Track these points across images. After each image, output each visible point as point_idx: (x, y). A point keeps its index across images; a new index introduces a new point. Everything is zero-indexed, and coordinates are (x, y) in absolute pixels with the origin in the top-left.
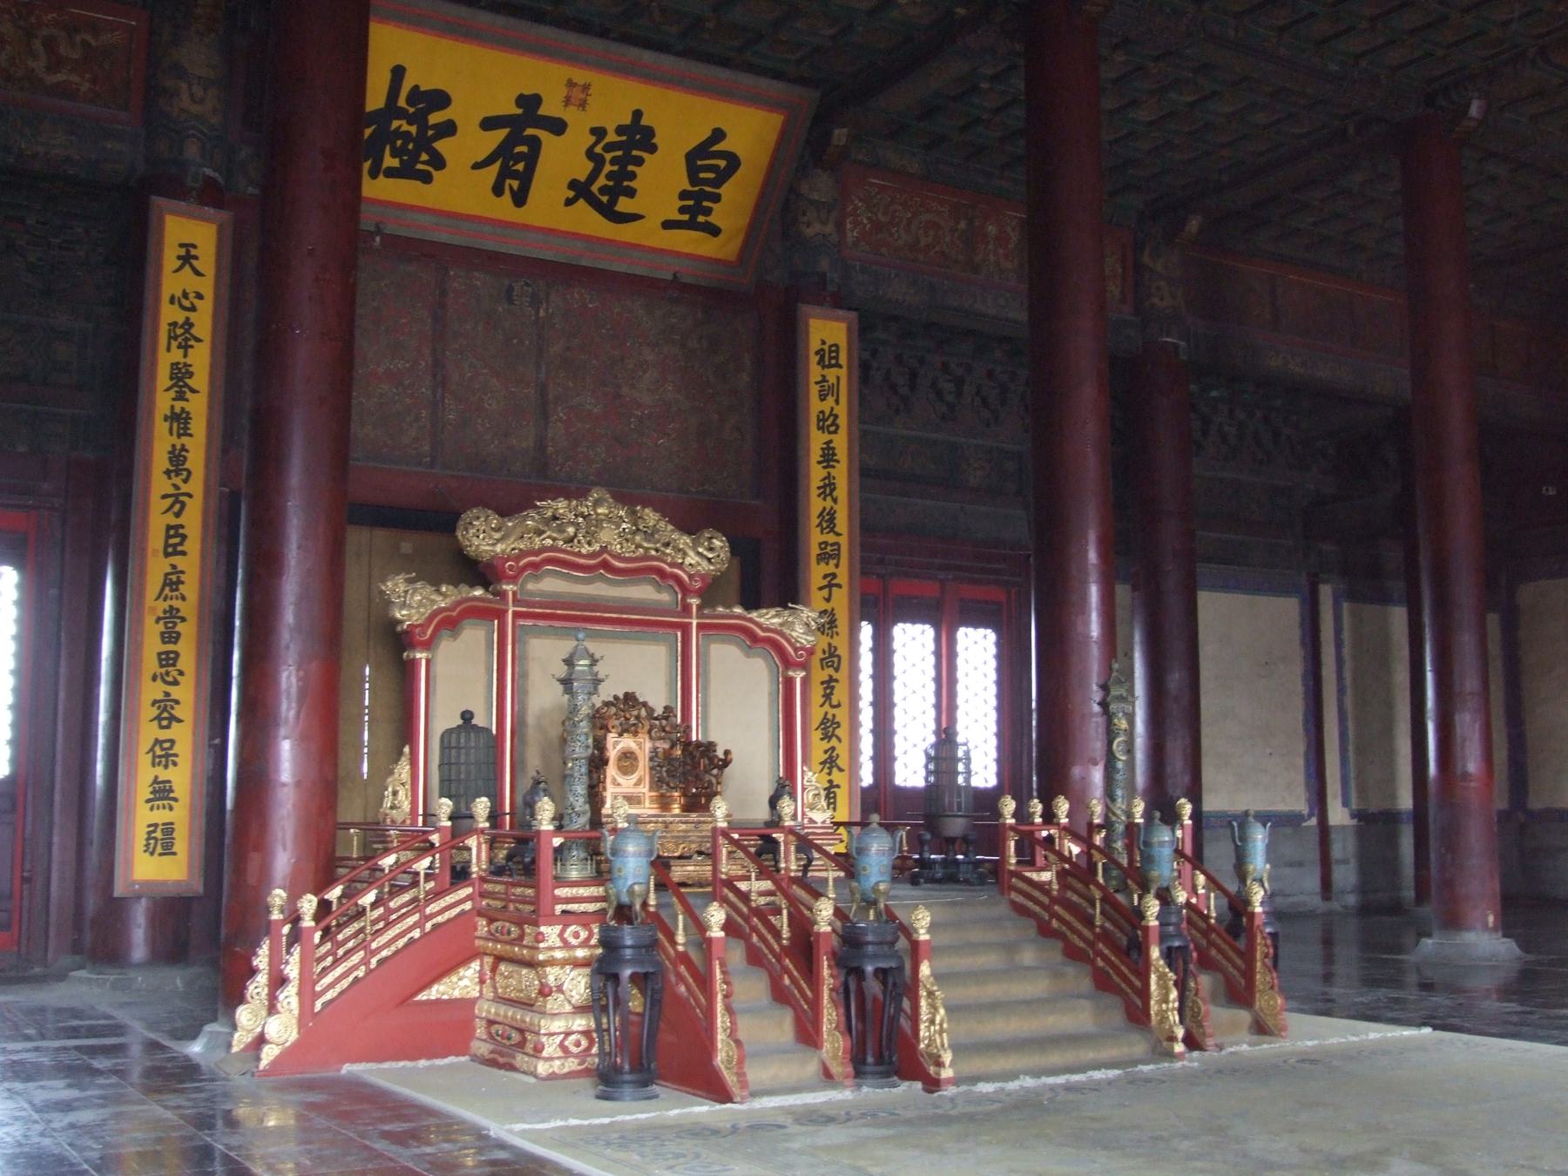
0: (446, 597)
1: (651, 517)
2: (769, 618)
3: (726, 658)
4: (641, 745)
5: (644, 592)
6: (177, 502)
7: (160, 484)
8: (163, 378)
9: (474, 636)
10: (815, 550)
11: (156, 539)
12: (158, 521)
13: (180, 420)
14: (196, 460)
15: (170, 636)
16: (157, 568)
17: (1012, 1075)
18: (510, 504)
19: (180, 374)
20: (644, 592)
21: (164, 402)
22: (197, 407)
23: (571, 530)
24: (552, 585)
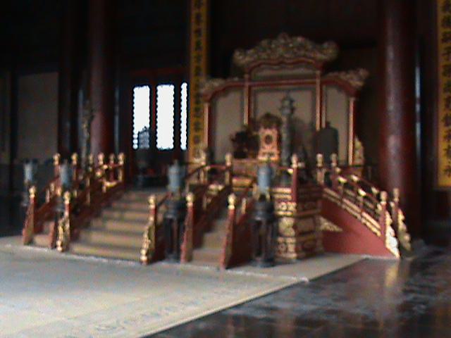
0: (217, 83)
1: (299, 39)
2: (344, 76)
3: (333, 94)
4: (272, 133)
5: (301, 71)
6: (198, 58)
7: (193, 54)
8: (193, 19)
9: (234, 97)
10: (440, 37)
11: (193, 71)
12: (193, 64)
13: (198, 32)
14: (203, 44)
15: (197, 102)
16: (193, 80)
17: (88, 255)
18: (246, 46)
19: (198, 16)
20: (301, 71)
21: (194, 27)
22: (203, 26)
23: (269, 51)
24: (267, 73)
